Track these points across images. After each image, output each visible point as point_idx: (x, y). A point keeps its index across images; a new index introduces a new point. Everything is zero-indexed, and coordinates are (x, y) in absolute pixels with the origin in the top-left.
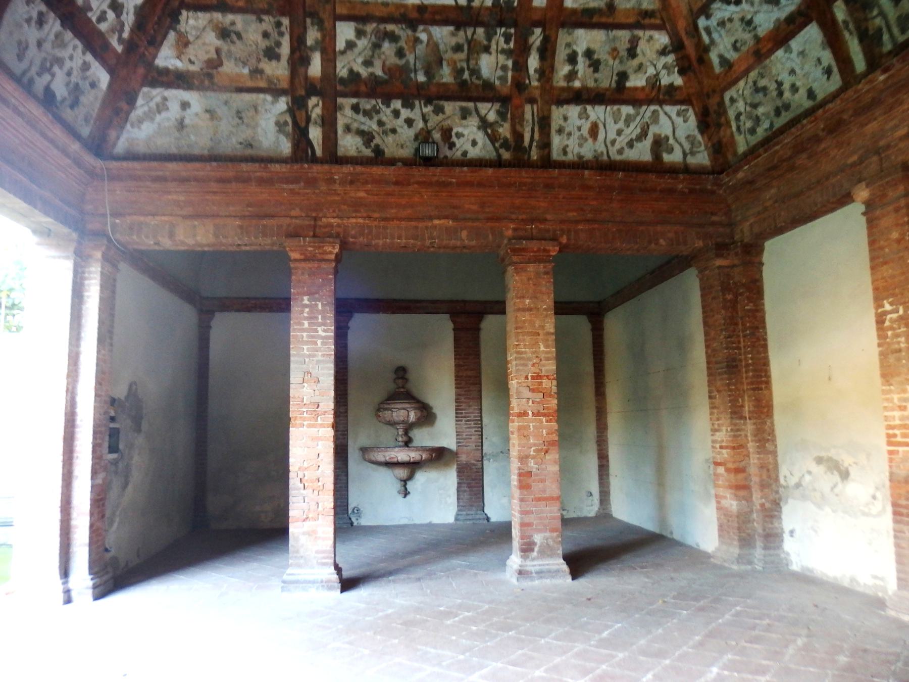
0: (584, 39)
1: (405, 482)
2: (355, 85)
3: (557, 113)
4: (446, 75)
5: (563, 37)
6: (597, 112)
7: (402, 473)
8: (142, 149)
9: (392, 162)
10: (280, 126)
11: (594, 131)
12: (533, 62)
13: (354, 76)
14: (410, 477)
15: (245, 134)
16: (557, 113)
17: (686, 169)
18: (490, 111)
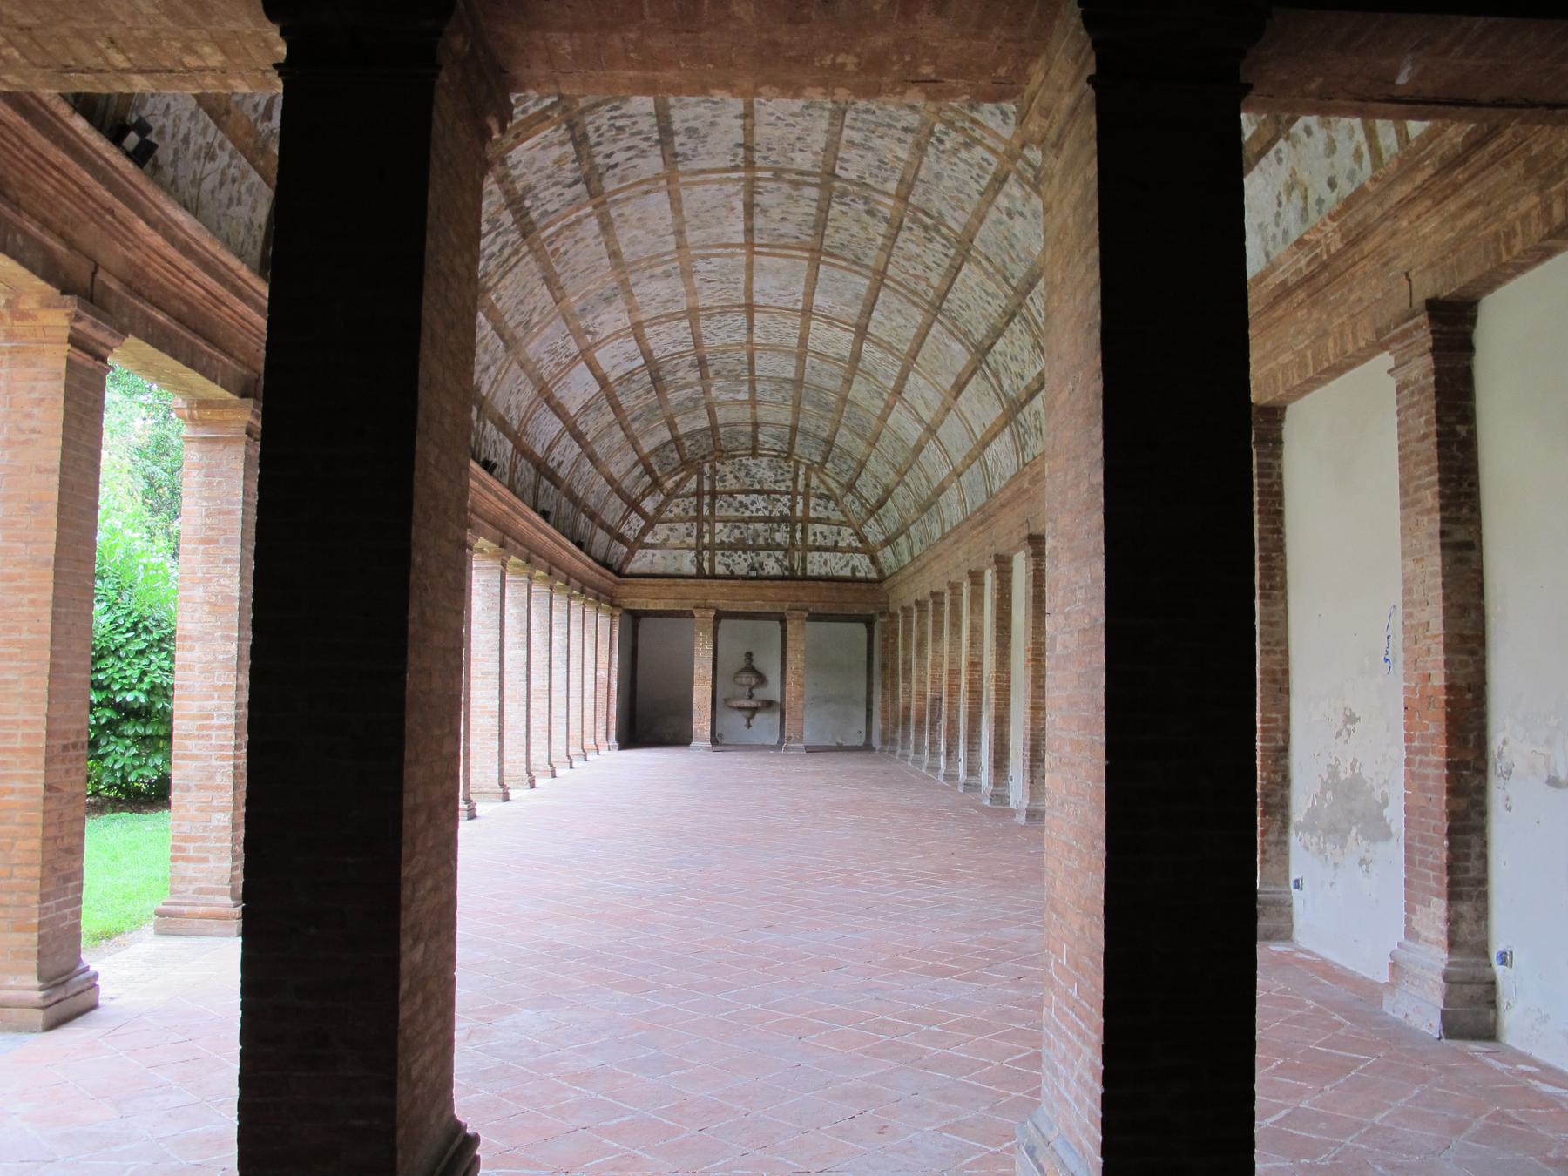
0: (818, 528)
1: (749, 720)
2: (722, 545)
3: (809, 555)
4: (761, 541)
5: (811, 528)
6: (826, 555)
7: (747, 713)
9: (736, 578)
11: (825, 563)
12: (798, 535)
13: (722, 542)
14: (753, 716)
15: (677, 565)
16: (809, 555)
17: (867, 581)
18: (780, 555)
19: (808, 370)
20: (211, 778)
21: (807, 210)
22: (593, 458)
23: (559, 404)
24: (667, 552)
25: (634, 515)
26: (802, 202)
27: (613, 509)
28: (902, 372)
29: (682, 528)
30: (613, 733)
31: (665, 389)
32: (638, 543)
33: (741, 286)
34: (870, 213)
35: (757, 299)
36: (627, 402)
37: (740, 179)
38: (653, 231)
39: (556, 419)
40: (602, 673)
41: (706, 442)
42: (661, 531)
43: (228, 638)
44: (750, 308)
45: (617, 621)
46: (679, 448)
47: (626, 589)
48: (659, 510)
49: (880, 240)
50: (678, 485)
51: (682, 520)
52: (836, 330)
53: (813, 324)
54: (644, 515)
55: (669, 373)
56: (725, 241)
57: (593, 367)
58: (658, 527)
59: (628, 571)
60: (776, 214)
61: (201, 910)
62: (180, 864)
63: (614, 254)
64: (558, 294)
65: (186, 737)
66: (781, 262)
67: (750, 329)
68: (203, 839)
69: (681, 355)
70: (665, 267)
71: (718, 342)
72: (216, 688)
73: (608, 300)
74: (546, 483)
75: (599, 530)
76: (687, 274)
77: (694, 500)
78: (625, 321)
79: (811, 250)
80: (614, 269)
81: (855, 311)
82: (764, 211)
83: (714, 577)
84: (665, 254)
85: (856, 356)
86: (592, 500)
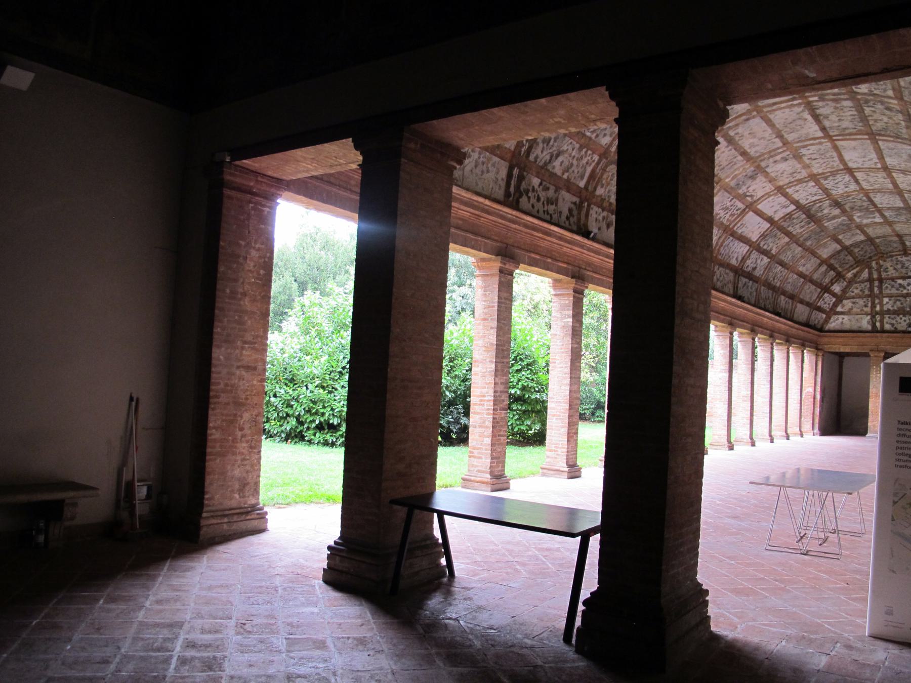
2: (888, 312)
8: (832, 329)
9: (899, 332)
10: (868, 323)
13: (889, 310)
15: (859, 325)
20: (484, 422)
21: (851, 113)
22: (782, 264)
24: (851, 316)
25: (826, 295)
26: (845, 110)
27: (810, 292)
29: (861, 302)
30: (817, 426)
31: (820, 221)
32: (832, 312)
33: (836, 159)
36: (796, 230)
37: (800, 104)
39: (742, 244)
40: (808, 389)
41: (869, 248)
42: (848, 304)
43: (491, 362)
45: (820, 359)
46: (851, 253)
47: (826, 340)
48: (844, 291)
50: (855, 275)
51: (860, 297)
54: (834, 295)
55: (817, 212)
56: (811, 136)
58: (845, 302)
59: (827, 328)
61: (478, 479)
62: (472, 459)
63: (744, 154)
65: (475, 404)
66: (853, 143)
68: (480, 449)
69: (820, 201)
71: (841, 192)
72: (487, 384)
73: (753, 177)
74: (744, 280)
75: (799, 305)
77: (868, 284)
79: (867, 134)
80: (747, 161)
83: (883, 331)
84: (778, 148)
86: (789, 288)
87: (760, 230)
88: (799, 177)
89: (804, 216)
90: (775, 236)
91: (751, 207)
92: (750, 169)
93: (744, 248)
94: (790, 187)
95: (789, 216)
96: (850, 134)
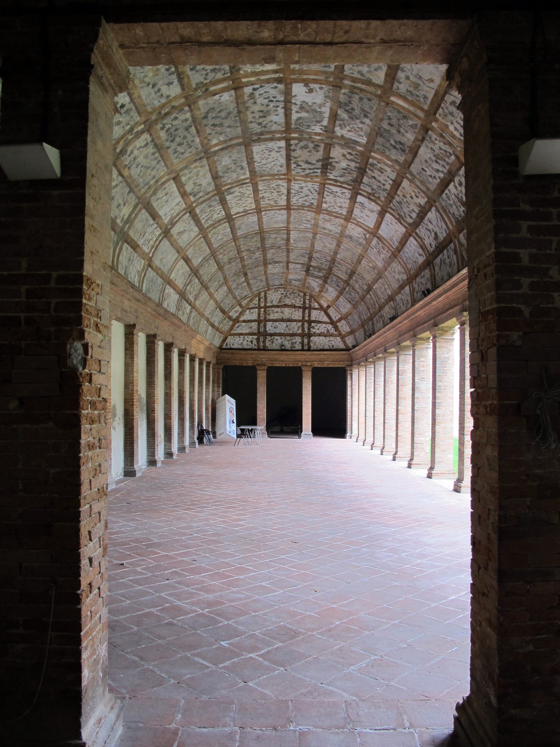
19: (245, 164)
23: (400, 243)
28: (201, 224)
33: (292, 217)
34: (248, 250)
35: (285, 212)
36: (388, 175)
38: (323, 242)
39: (408, 244)
44: (288, 207)
49: (242, 247)
52: (241, 210)
53: (254, 207)
57: (378, 225)
60: (278, 239)
63: (338, 246)
64: (361, 257)
67: (289, 193)
70: (324, 231)
71: (310, 185)
73: (351, 237)
76: (316, 225)
78: (350, 226)
80: (342, 243)
81: (237, 223)
82: (283, 239)
85: (223, 202)
87: (394, 223)
88: (327, 217)
89: (365, 180)
90: (400, 203)
91: (374, 232)
92: (345, 240)
93: (412, 242)
94: (341, 214)
95: (371, 197)
96: (274, 230)
